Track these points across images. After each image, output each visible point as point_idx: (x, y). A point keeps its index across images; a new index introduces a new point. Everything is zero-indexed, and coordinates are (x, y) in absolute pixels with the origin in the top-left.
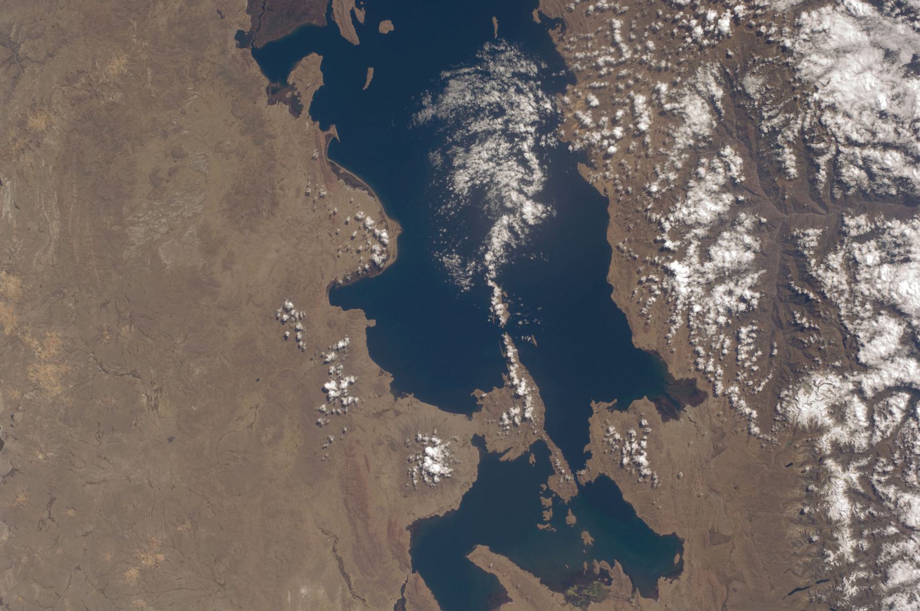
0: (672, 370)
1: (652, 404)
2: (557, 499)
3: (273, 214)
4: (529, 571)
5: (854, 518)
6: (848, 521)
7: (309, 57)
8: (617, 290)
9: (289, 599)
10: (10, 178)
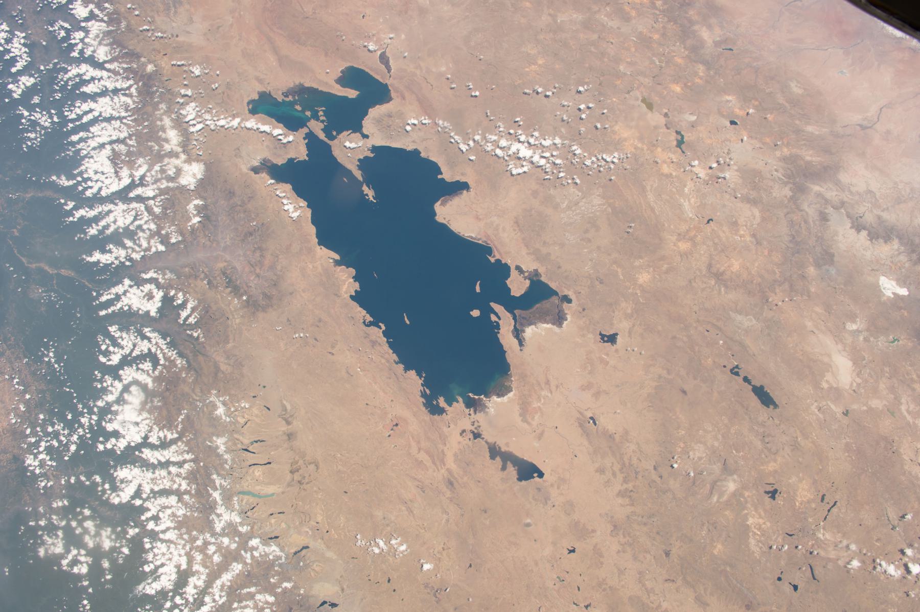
1: (275, 162)
2: (317, 119)
3: (515, 218)
4: (325, 92)
5: (164, 131)
6: (168, 131)
10: (691, 218)
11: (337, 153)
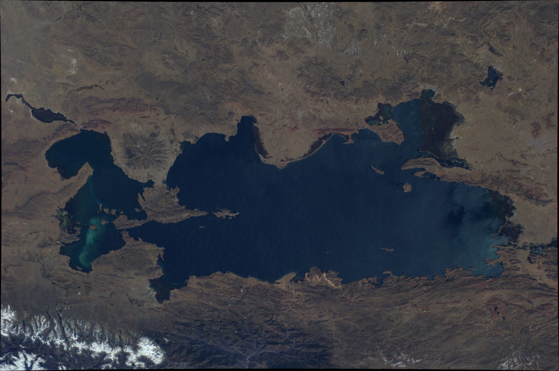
0: (176, 291)
1: (159, 277)
2: (114, 217)
3: (306, 92)
4: (77, 194)
5: (92, 352)
6: (91, 349)
7: (402, 136)
8: (222, 275)
9: (70, 50)
11: (164, 220)
